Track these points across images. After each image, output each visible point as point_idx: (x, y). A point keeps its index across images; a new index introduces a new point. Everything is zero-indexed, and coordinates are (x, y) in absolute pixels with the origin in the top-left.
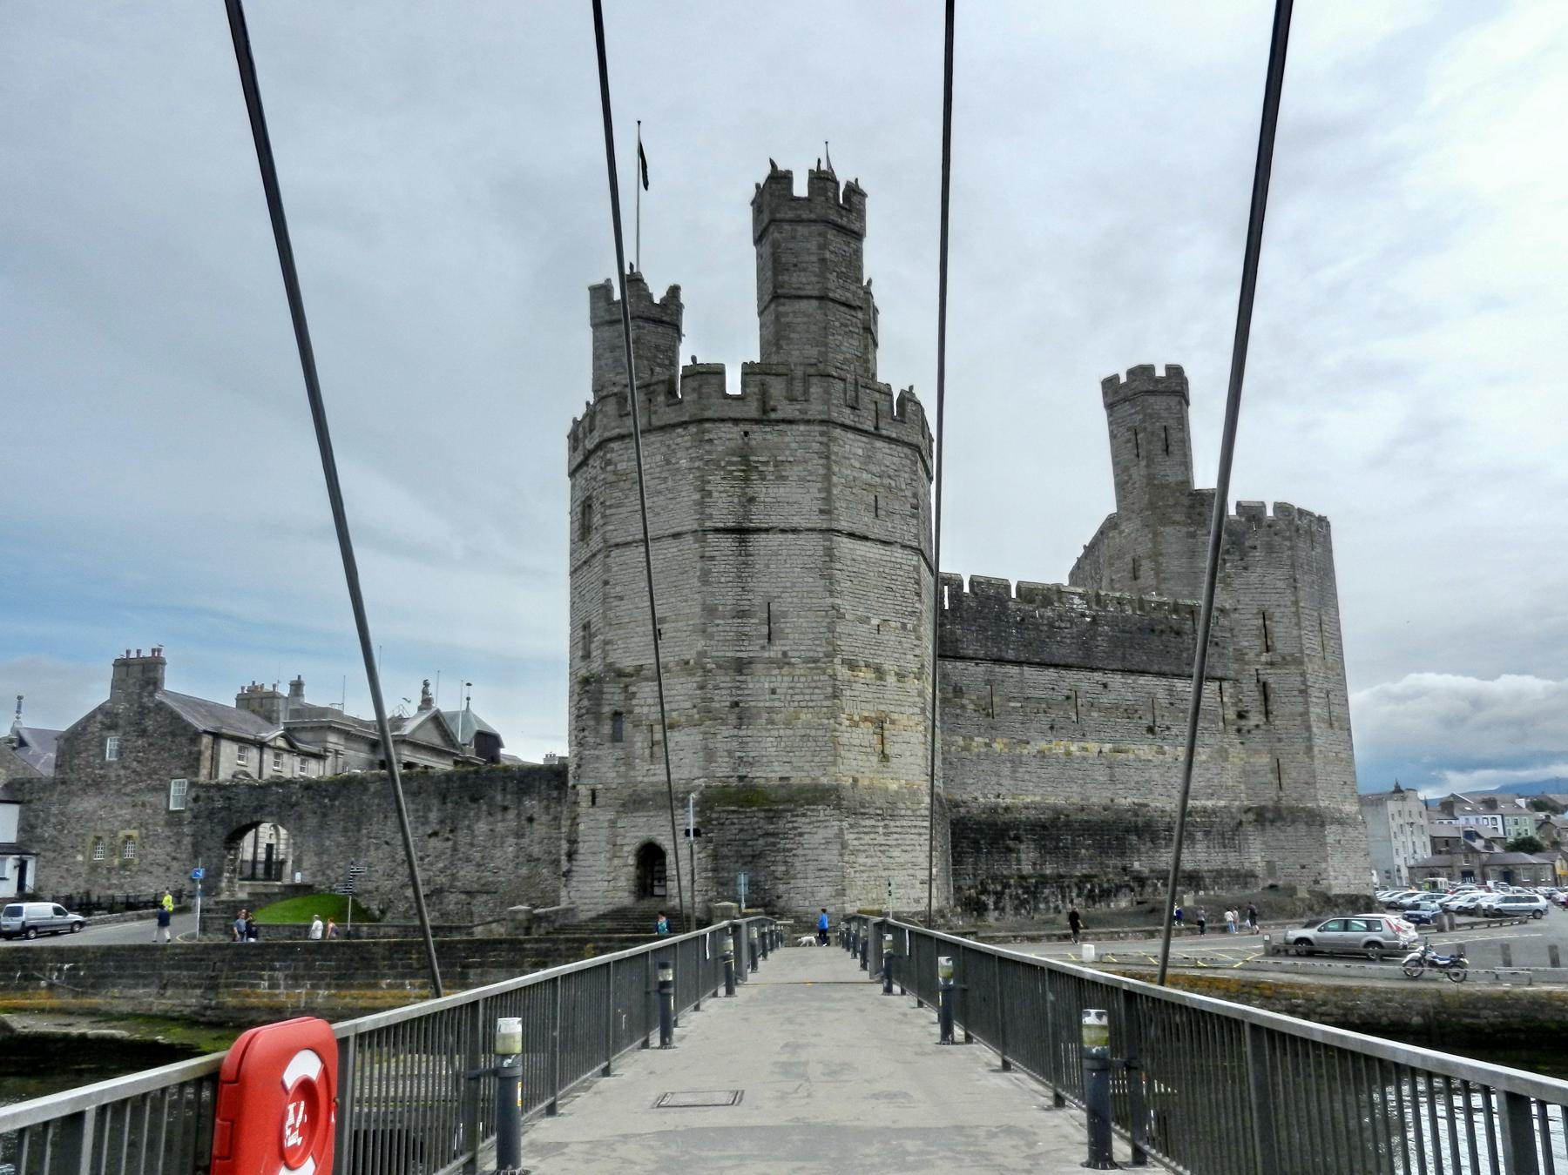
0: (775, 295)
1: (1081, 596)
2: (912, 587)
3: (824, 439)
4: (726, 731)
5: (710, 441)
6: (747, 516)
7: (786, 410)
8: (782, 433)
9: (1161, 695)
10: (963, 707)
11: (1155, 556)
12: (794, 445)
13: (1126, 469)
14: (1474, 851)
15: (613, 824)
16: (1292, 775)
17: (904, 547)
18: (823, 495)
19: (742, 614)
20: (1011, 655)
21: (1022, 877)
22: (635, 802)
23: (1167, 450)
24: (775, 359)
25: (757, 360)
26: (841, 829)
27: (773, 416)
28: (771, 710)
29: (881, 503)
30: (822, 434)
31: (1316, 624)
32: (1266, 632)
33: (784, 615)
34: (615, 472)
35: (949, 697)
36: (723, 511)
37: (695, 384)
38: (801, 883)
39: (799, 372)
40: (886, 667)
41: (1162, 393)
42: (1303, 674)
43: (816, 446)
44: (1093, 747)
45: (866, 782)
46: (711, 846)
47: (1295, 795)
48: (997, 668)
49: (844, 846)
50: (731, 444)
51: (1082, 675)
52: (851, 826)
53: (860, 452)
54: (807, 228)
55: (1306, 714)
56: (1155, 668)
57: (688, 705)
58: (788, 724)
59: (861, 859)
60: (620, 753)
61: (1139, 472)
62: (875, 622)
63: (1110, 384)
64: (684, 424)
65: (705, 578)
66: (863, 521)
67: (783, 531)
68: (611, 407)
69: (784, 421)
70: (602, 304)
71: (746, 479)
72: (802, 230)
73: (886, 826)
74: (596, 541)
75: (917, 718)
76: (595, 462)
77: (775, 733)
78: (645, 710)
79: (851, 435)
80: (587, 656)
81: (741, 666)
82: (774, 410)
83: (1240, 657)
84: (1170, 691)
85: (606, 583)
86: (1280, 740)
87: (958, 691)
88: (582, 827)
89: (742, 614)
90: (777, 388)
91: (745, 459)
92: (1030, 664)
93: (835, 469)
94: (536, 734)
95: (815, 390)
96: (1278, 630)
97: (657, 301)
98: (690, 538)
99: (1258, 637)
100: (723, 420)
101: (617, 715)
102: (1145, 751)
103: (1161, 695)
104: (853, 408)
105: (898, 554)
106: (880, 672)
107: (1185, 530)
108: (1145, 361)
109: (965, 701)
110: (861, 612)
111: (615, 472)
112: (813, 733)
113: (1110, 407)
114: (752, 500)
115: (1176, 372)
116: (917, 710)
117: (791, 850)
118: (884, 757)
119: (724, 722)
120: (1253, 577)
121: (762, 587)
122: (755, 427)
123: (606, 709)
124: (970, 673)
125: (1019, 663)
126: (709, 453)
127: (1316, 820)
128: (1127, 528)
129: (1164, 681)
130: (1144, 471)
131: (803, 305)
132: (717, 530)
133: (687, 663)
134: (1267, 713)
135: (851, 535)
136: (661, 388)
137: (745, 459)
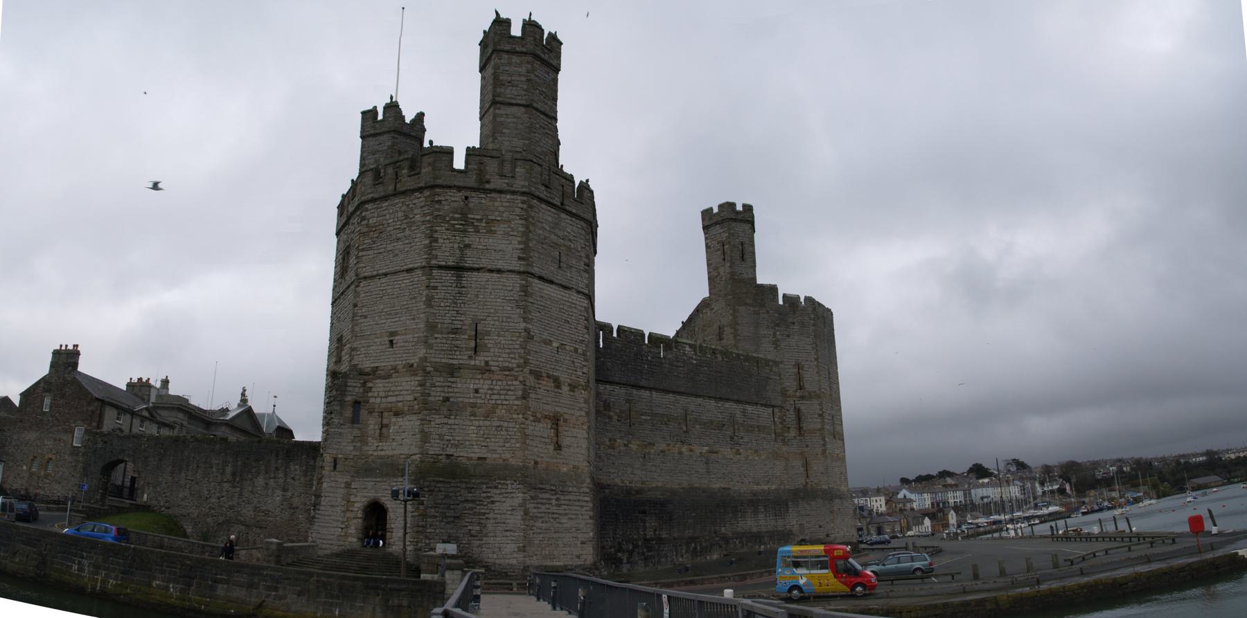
0: (493, 103)
1: (690, 346)
3: (525, 206)
4: (438, 419)
5: (439, 202)
6: (462, 257)
8: (493, 199)
9: (738, 415)
10: (610, 417)
11: (734, 324)
12: (502, 209)
13: (716, 269)
14: (864, 517)
15: (348, 485)
17: (579, 292)
18: (522, 246)
19: (455, 331)
20: (643, 383)
21: (646, 540)
22: (367, 470)
23: (743, 258)
24: (490, 146)
25: (477, 146)
26: (524, 500)
27: (487, 186)
28: (474, 405)
29: (563, 258)
30: (523, 202)
32: (800, 378)
33: (488, 333)
34: (368, 226)
35: (602, 409)
36: (447, 253)
37: (431, 160)
38: (491, 540)
39: (508, 156)
40: (561, 379)
41: (741, 221)
43: (518, 211)
44: (698, 450)
46: (422, 507)
48: (635, 392)
50: (455, 205)
52: (533, 498)
53: (550, 219)
54: (521, 65)
55: (822, 429)
56: (735, 397)
57: (411, 398)
58: (487, 416)
59: (539, 524)
60: (356, 432)
61: (724, 271)
62: (555, 344)
63: (707, 214)
64: (420, 190)
65: (429, 302)
66: (550, 270)
67: (491, 271)
68: (369, 179)
69: (495, 191)
70: (370, 123)
71: (465, 231)
74: (351, 276)
75: (583, 419)
76: (355, 220)
77: (476, 423)
78: (378, 400)
79: (543, 206)
80: (339, 361)
81: (452, 371)
82: (488, 182)
83: (784, 393)
84: (744, 412)
85: (355, 306)
87: (607, 406)
88: (325, 485)
90: (492, 166)
91: (464, 216)
92: (657, 390)
93: (532, 228)
94: (308, 426)
95: (520, 170)
97: (408, 121)
98: (419, 272)
100: (450, 187)
101: (357, 403)
102: (726, 451)
104: (547, 187)
105: (575, 297)
106: (557, 383)
108: (731, 200)
110: (546, 336)
111: (368, 226)
112: (505, 424)
113: (706, 228)
114: (468, 246)
115: (748, 209)
116: (583, 413)
117: (484, 514)
118: (558, 447)
119: (437, 411)
122: (473, 194)
123: (348, 398)
124: (617, 393)
125: (650, 389)
126: (438, 210)
128: (716, 307)
129: (740, 406)
130: (728, 270)
131: (514, 109)
132: (440, 267)
133: (412, 366)
134: (800, 429)
135: (541, 278)
136: (406, 164)
137: (464, 216)
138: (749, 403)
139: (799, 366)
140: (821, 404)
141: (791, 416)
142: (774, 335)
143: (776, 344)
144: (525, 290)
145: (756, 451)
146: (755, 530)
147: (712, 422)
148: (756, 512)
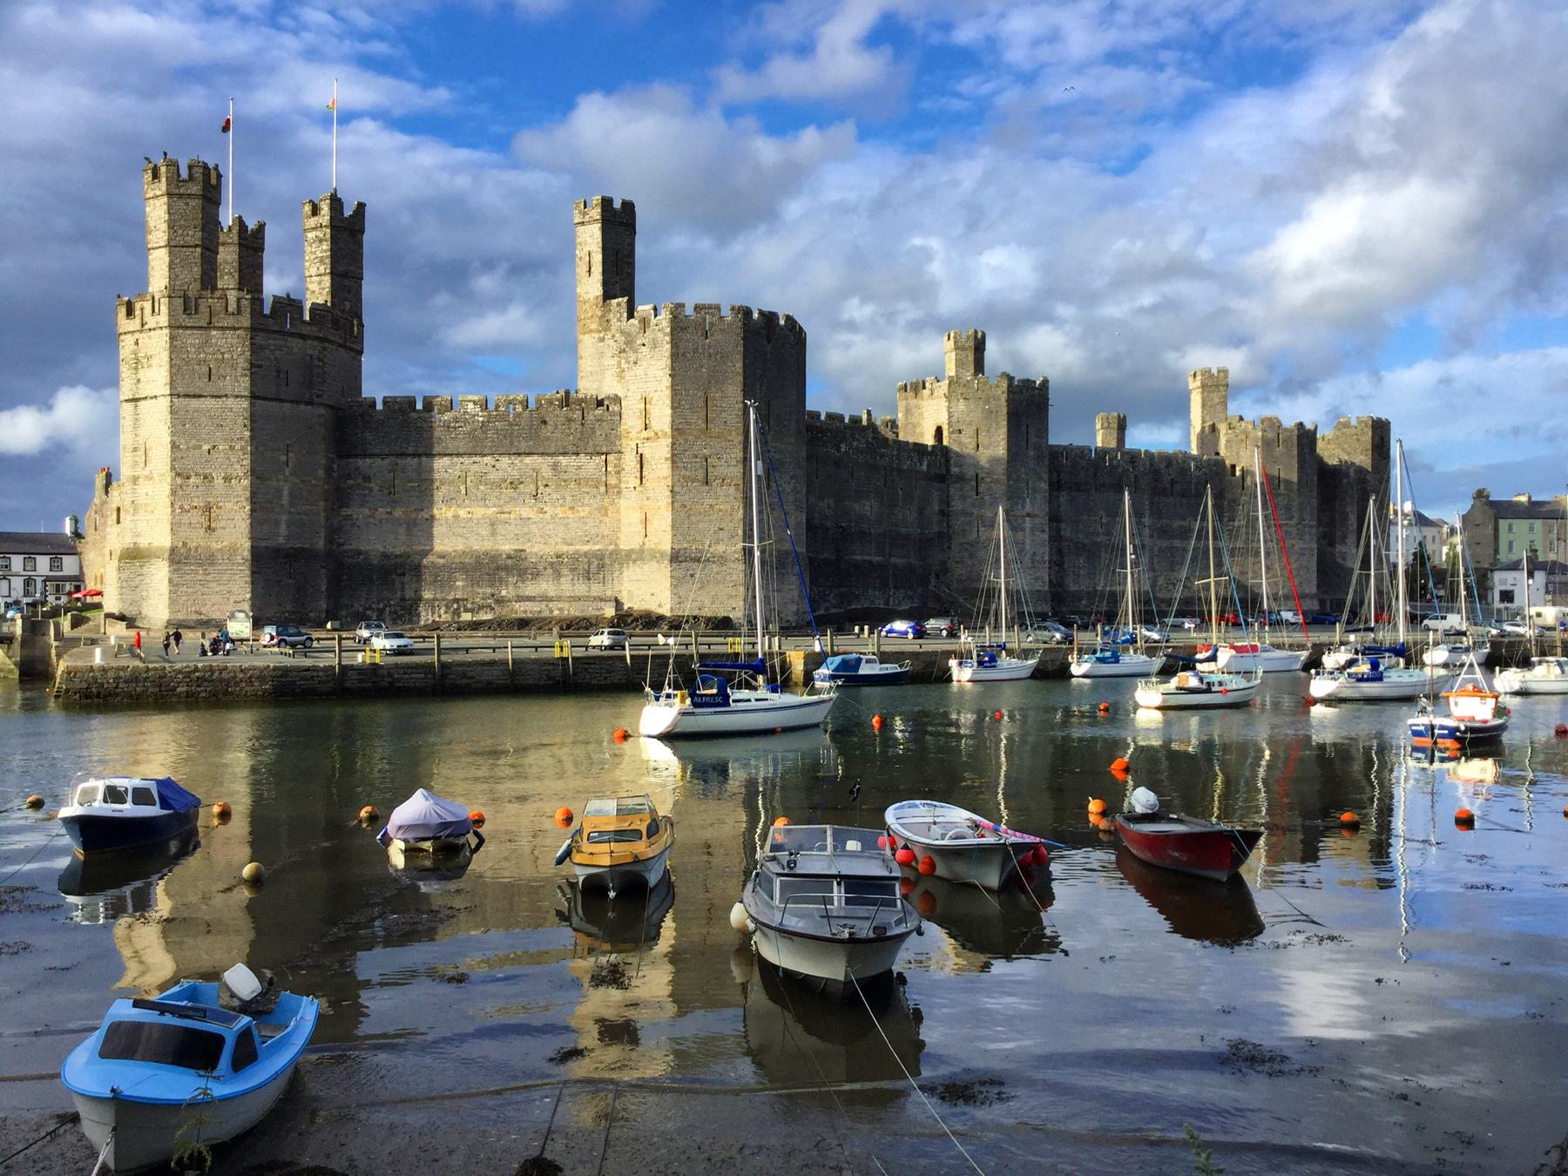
1: (475, 403)
2: (240, 421)
10: (370, 489)
20: (411, 450)
21: (403, 599)
44: (479, 512)
62: (206, 447)
66: (200, 385)
84: (555, 467)
87: (367, 479)
89: (135, 449)
102: (526, 512)
103: (546, 472)
120: (639, 370)
121: (143, 432)
125: (419, 455)
135: (188, 396)
138: (565, 454)
141: (630, 461)
143: (621, 374)
145: (572, 508)
146: (551, 594)
148: (558, 575)
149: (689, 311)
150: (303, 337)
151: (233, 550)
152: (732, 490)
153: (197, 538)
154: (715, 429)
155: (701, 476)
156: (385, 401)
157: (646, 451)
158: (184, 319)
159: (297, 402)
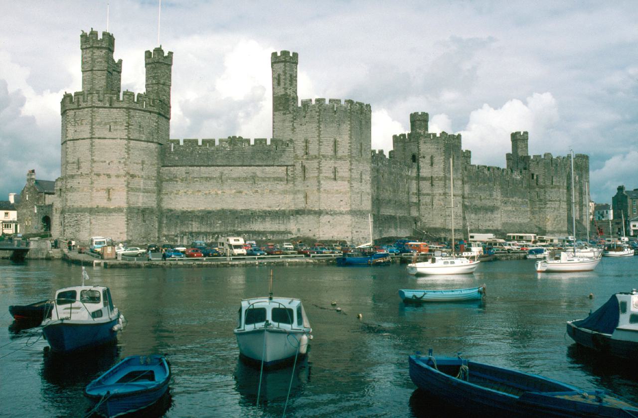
2: (124, 150)
7: (83, 105)
9: (259, 174)
10: (177, 181)
16: (312, 198)
17: (121, 139)
20: (196, 164)
27: (80, 107)
28: (79, 188)
31: (332, 143)
42: (319, 163)
44: (228, 192)
45: (102, 206)
47: (311, 206)
48: (190, 168)
49: (91, 223)
51: (225, 168)
52: (94, 218)
59: (97, 227)
62: (108, 162)
72: (88, 51)
73: (107, 218)
81: (72, 177)
82: (80, 105)
83: (296, 157)
86: (308, 186)
96: (311, 146)
99: (303, 150)
100: (70, 110)
105: (119, 141)
106: (109, 176)
107: (282, 112)
109: (177, 179)
110: (102, 159)
114: (76, 131)
118: (109, 199)
122: (77, 111)
126: (68, 119)
127: (319, 213)
135: (99, 138)
139: (306, 141)
140: (319, 163)
142: (293, 125)
143: (293, 129)
144: (91, 144)
146: (262, 230)
147: (239, 178)
149: (327, 102)
150: (150, 112)
151: (119, 210)
152: (347, 182)
153: (103, 203)
154: (340, 154)
155: (333, 177)
156: (185, 141)
157: (307, 164)
158: (100, 104)
159: (148, 141)
